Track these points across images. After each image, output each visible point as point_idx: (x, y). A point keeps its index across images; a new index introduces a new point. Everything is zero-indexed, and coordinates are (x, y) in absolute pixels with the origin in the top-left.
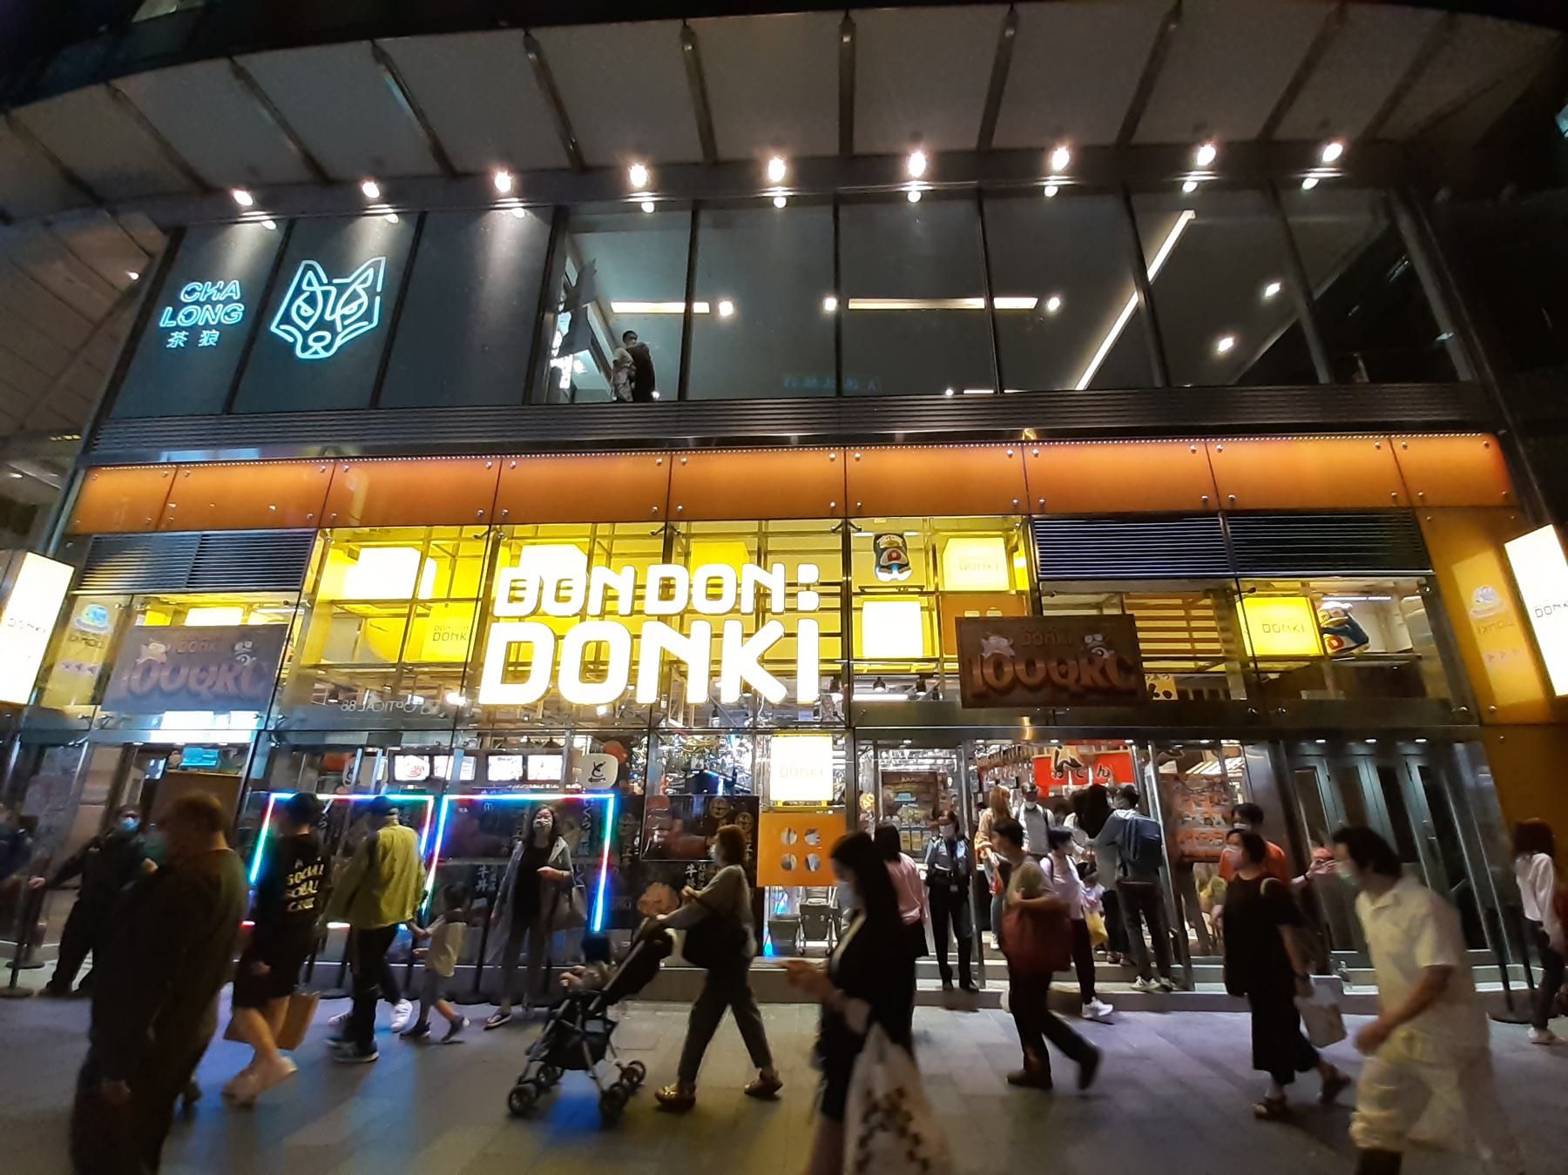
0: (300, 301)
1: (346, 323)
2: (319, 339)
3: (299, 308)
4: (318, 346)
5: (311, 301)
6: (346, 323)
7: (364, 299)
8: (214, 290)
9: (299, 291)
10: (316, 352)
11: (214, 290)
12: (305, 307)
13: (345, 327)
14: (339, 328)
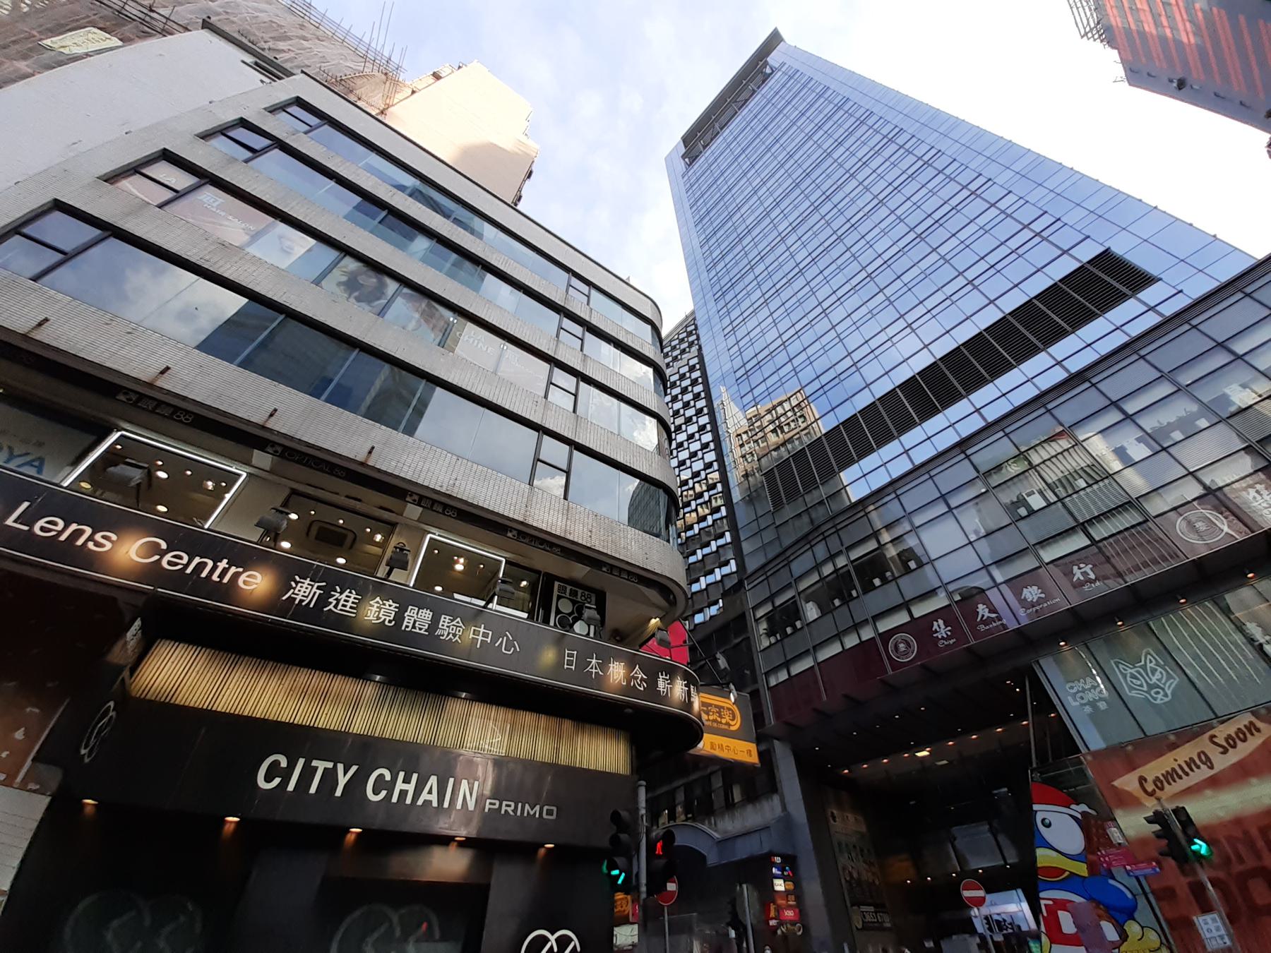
0: (1129, 679)
1: (1163, 682)
2: (1158, 693)
3: (1132, 682)
4: (1160, 696)
5: (1133, 676)
6: (1163, 682)
7: (1159, 669)
8: (1081, 685)
9: (1125, 676)
10: (1162, 699)
11: (1081, 685)
12: (1134, 681)
13: (1164, 684)
14: (1162, 686)
